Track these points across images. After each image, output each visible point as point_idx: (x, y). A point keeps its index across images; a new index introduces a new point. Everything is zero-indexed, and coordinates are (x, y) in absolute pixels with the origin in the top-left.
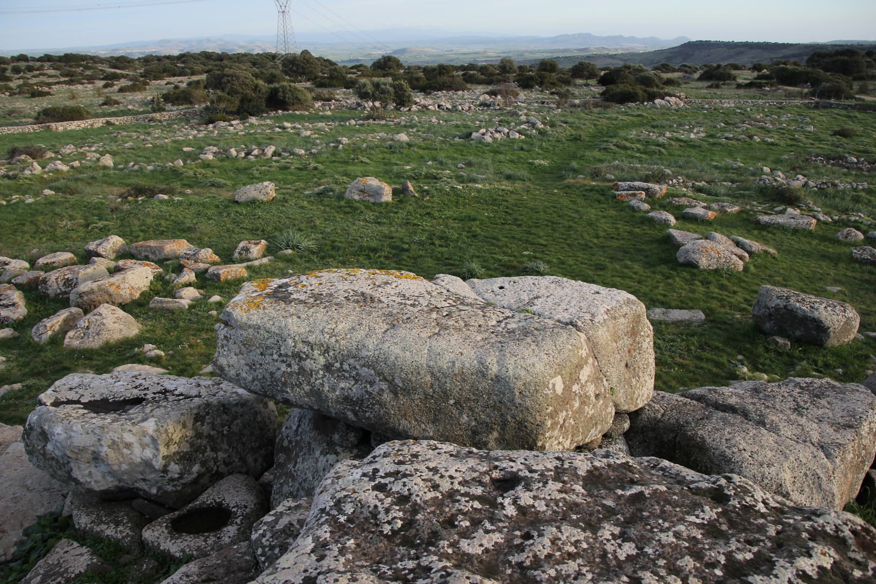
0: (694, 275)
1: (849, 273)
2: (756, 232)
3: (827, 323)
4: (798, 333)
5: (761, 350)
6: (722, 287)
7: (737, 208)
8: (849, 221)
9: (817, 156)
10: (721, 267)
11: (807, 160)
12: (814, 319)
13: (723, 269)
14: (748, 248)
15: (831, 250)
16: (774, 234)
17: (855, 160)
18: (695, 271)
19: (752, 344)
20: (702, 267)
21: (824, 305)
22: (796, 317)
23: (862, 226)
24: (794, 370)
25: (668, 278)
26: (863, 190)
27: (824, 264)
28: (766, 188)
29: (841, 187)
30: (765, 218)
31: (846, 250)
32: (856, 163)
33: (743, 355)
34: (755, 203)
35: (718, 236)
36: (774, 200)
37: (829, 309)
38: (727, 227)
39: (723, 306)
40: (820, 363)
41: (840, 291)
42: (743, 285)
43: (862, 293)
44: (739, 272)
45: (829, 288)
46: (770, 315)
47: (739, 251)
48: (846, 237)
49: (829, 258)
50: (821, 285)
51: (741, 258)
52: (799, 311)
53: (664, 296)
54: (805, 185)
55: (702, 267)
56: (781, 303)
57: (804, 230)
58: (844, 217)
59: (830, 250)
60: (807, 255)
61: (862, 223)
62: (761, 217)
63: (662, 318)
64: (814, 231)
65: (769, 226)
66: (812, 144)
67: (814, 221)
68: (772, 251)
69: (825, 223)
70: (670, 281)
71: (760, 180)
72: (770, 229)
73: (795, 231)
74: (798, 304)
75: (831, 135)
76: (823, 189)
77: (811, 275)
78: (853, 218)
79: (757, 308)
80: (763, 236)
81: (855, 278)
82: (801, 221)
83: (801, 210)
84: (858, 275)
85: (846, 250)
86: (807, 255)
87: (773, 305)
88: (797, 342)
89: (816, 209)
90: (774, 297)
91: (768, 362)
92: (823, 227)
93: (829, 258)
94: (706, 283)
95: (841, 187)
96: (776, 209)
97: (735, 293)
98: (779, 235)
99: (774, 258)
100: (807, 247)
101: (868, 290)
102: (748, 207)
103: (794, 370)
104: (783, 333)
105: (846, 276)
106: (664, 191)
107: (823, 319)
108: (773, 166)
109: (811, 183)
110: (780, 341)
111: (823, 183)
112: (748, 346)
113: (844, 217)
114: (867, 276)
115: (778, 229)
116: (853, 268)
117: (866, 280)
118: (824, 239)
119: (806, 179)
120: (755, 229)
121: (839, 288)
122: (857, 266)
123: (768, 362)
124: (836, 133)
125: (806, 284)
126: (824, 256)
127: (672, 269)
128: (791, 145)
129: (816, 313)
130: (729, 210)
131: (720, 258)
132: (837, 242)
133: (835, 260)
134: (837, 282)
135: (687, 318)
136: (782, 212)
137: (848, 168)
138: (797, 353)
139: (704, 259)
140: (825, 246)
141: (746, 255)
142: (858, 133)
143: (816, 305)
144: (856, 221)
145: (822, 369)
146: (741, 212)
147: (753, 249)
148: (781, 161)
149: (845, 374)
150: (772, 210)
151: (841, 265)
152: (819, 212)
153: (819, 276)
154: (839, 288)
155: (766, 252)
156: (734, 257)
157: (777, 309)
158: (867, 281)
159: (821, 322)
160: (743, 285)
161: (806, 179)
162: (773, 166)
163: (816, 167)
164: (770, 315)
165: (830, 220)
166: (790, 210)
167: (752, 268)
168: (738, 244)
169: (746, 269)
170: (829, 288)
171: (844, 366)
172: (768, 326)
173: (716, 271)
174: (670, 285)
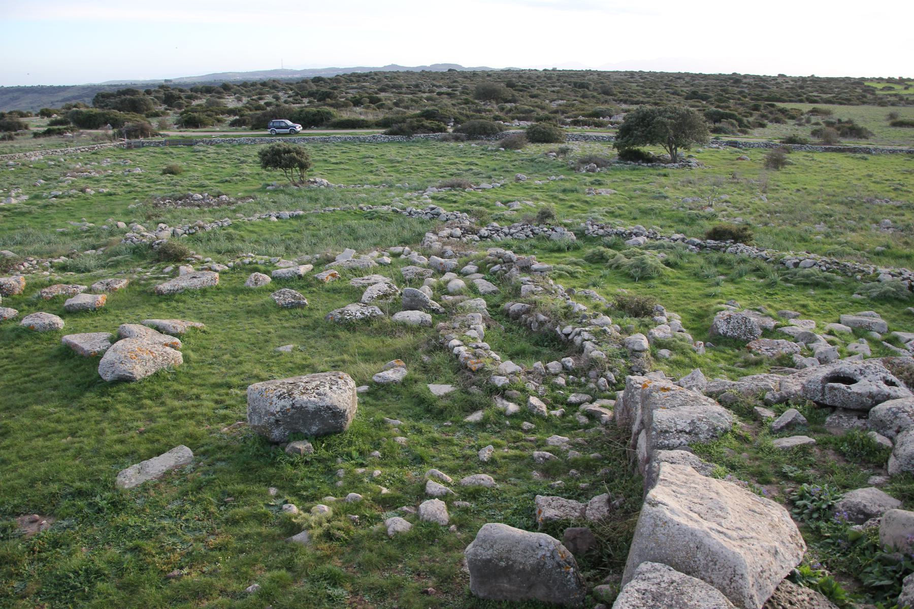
0: (134, 392)
1: (286, 325)
2: (163, 305)
3: (342, 406)
4: (314, 429)
5: (289, 470)
6: (177, 395)
7: (124, 282)
8: (244, 264)
9: (164, 199)
10: (160, 368)
11: (156, 205)
12: (327, 407)
13: (163, 370)
14: (174, 331)
15: (253, 302)
16: (184, 302)
17: (201, 197)
18: (132, 385)
19: (272, 465)
20: (138, 377)
21: (328, 386)
22: (308, 412)
23: (259, 266)
24: (340, 479)
25: (106, 410)
26: (229, 226)
27: (256, 321)
28: (138, 247)
29: (209, 228)
30: (166, 286)
31: (266, 298)
32: (203, 199)
33: (275, 486)
34: (139, 269)
35: (135, 328)
36: (158, 261)
37: (334, 388)
38: (127, 308)
39: (199, 423)
40: (355, 454)
41: (294, 349)
42: (196, 381)
43: (312, 342)
44: (181, 366)
45: (281, 349)
46: (277, 421)
47: (168, 339)
48: (256, 284)
49: (256, 312)
50: (272, 349)
51: (173, 346)
52: (309, 405)
53: (122, 442)
54: (174, 234)
55: (138, 377)
56: (287, 403)
57: (211, 287)
58: (238, 261)
59: (250, 302)
60: (233, 316)
61: (257, 263)
62: (161, 287)
63: (142, 479)
64: (220, 286)
65: (174, 294)
66: (149, 187)
67: (217, 275)
68: (198, 324)
69: (224, 273)
70: (112, 414)
71: (126, 239)
72: (177, 297)
73: (204, 292)
74: (305, 397)
75: (161, 175)
76: (193, 234)
77: (253, 340)
78: (247, 261)
79: (256, 418)
80: (174, 308)
81: (294, 328)
82: (204, 279)
83: (192, 264)
84: (294, 323)
85: (266, 298)
86: (233, 316)
87: (278, 409)
88: (318, 438)
89: (206, 260)
90: (275, 399)
91: (307, 482)
92: (224, 277)
93: (256, 312)
94: (156, 397)
95: (209, 228)
96: (167, 270)
97: (198, 397)
98: (191, 302)
99: (204, 332)
100: (225, 307)
101: (314, 337)
102: (135, 276)
103: (340, 479)
104: (298, 436)
105: (285, 327)
106: (24, 283)
107: (336, 404)
108: (127, 219)
109: (180, 231)
110: (302, 446)
111: (190, 228)
112: (272, 471)
113: (238, 261)
114: (303, 322)
115: (185, 294)
116: (285, 316)
117: (305, 326)
118: (236, 291)
119: (172, 228)
120: (160, 302)
121: (292, 346)
122: (286, 312)
123: (307, 482)
124: (165, 172)
125: (257, 353)
126: (250, 312)
127: (102, 394)
128: (130, 192)
129: (327, 399)
130: (117, 287)
131: (155, 357)
132: (249, 291)
133: (263, 312)
134: (283, 338)
135: (172, 463)
136: (175, 274)
137: (198, 206)
138: (323, 453)
139: (137, 367)
140: (242, 299)
141: (177, 340)
142: (185, 169)
143: (321, 390)
144: (250, 263)
145: (361, 461)
146: (132, 284)
147: (179, 330)
148: (132, 212)
149: (384, 454)
150: (162, 272)
151: (273, 317)
152: (211, 262)
153: (262, 338)
154: (292, 346)
155: (194, 328)
156: (168, 348)
157: (284, 412)
158: (306, 327)
159: (336, 407)
160: (196, 381)
161: (172, 228)
162: (127, 219)
163: (169, 211)
164: (277, 421)
165: (227, 268)
166: (183, 268)
167: (193, 356)
168: (159, 329)
169: (186, 359)
170: (281, 349)
171: (377, 446)
172: (276, 434)
173: (157, 375)
174: (115, 420)
